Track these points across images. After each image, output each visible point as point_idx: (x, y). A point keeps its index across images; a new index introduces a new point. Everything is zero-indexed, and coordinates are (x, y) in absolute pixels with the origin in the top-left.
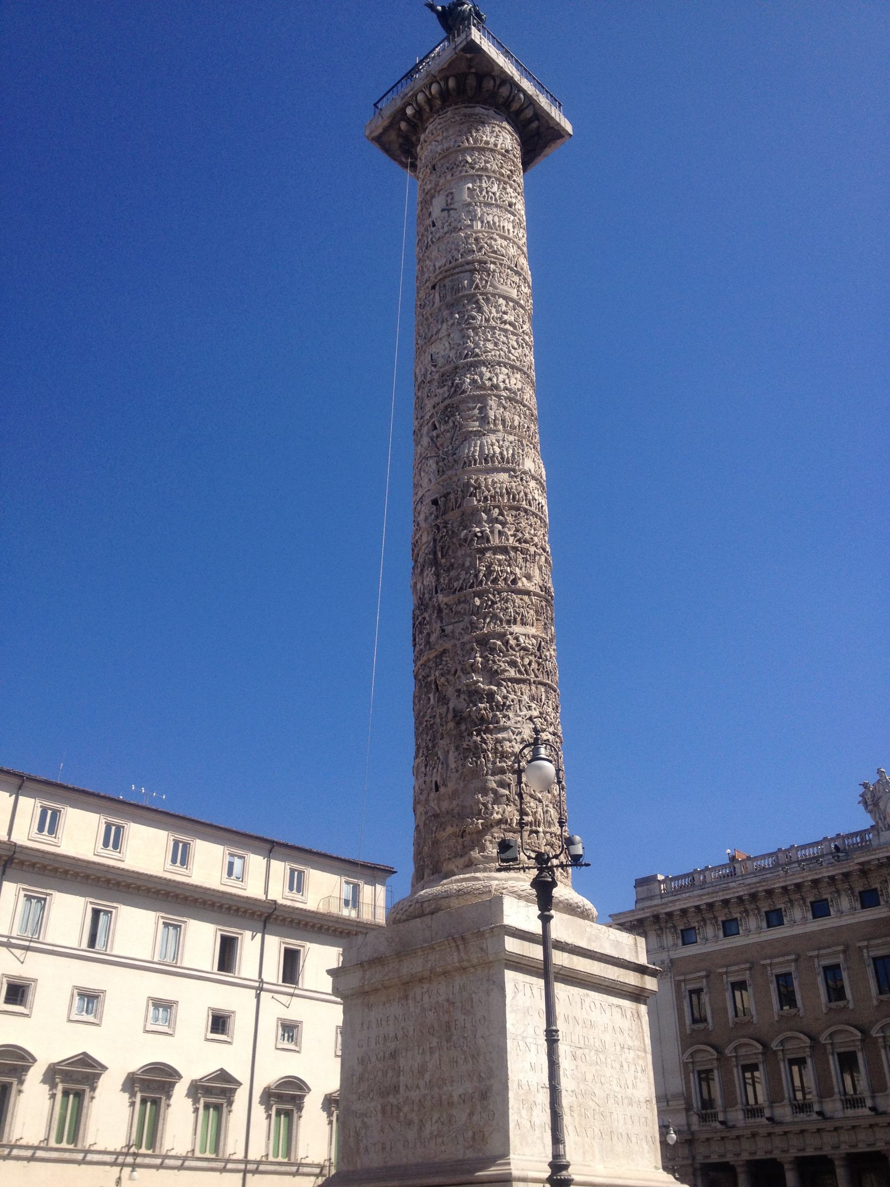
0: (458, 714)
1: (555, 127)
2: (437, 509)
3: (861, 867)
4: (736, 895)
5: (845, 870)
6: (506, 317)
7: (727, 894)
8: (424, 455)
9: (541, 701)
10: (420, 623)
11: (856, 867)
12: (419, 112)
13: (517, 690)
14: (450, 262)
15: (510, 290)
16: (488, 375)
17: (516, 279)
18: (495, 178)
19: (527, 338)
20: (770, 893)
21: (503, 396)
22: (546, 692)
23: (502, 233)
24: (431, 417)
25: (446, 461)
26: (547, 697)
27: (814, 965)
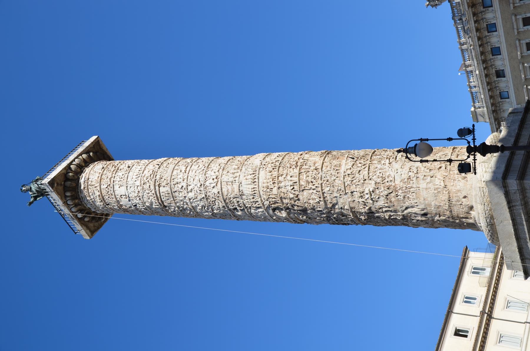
0: (386, 202)
1: (94, 144)
3: (470, 7)
4: (483, 70)
5: (472, 15)
6: (183, 171)
7: (482, 75)
8: (249, 215)
9: (381, 158)
10: (337, 221)
11: (470, 9)
12: (81, 211)
13: (375, 170)
14: (154, 198)
15: (170, 168)
16: (211, 181)
17: (165, 165)
18: (115, 174)
19: (194, 161)
20: (482, 53)
22: (376, 155)
23: (142, 171)
25: (253, 203)
26: (378, 155)
27: (522, 31)
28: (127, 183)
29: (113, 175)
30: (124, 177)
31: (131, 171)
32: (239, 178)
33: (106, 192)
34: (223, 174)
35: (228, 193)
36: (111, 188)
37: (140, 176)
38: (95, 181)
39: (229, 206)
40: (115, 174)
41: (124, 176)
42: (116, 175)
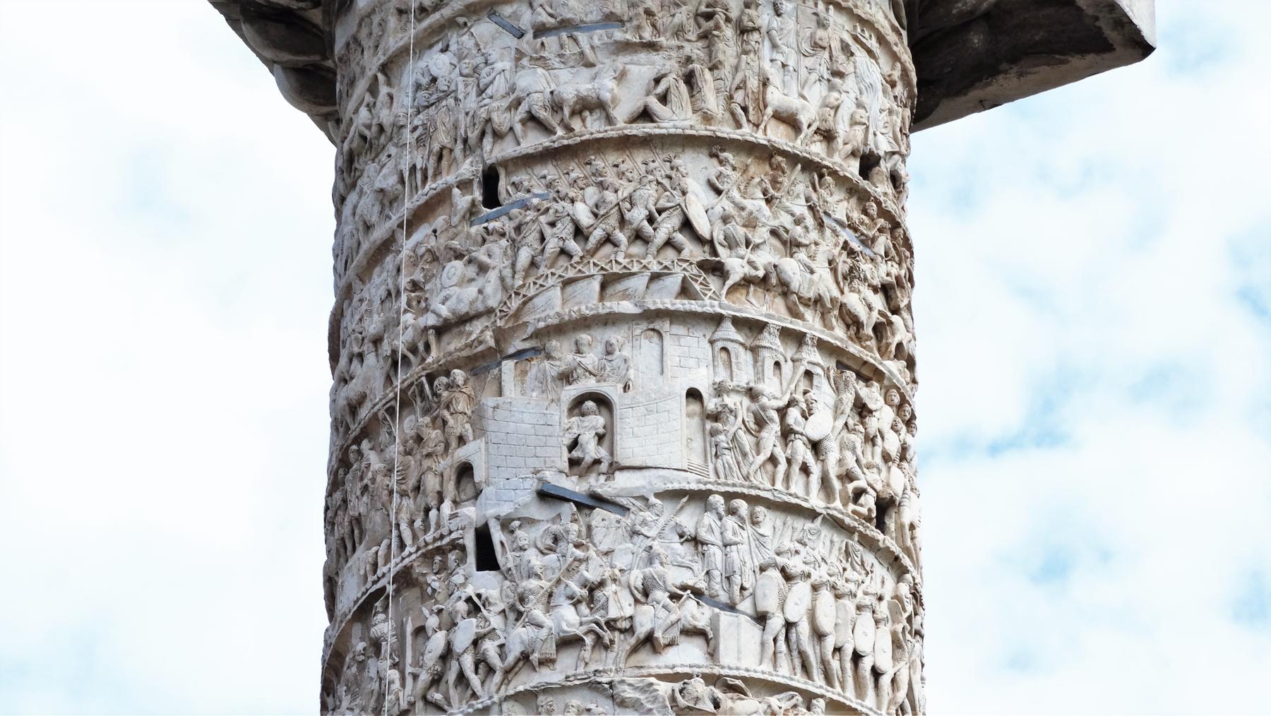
18: (822, 345)
28: (742, 505)
29: (811, 324)
30: (796, 468)
31: (854, 544)
33: (638, 216)
36: (685, 291)
37: (806, 668)
38: (753, 83)
40: (822, 345)
41: (805, 469)
42: (812, 355)
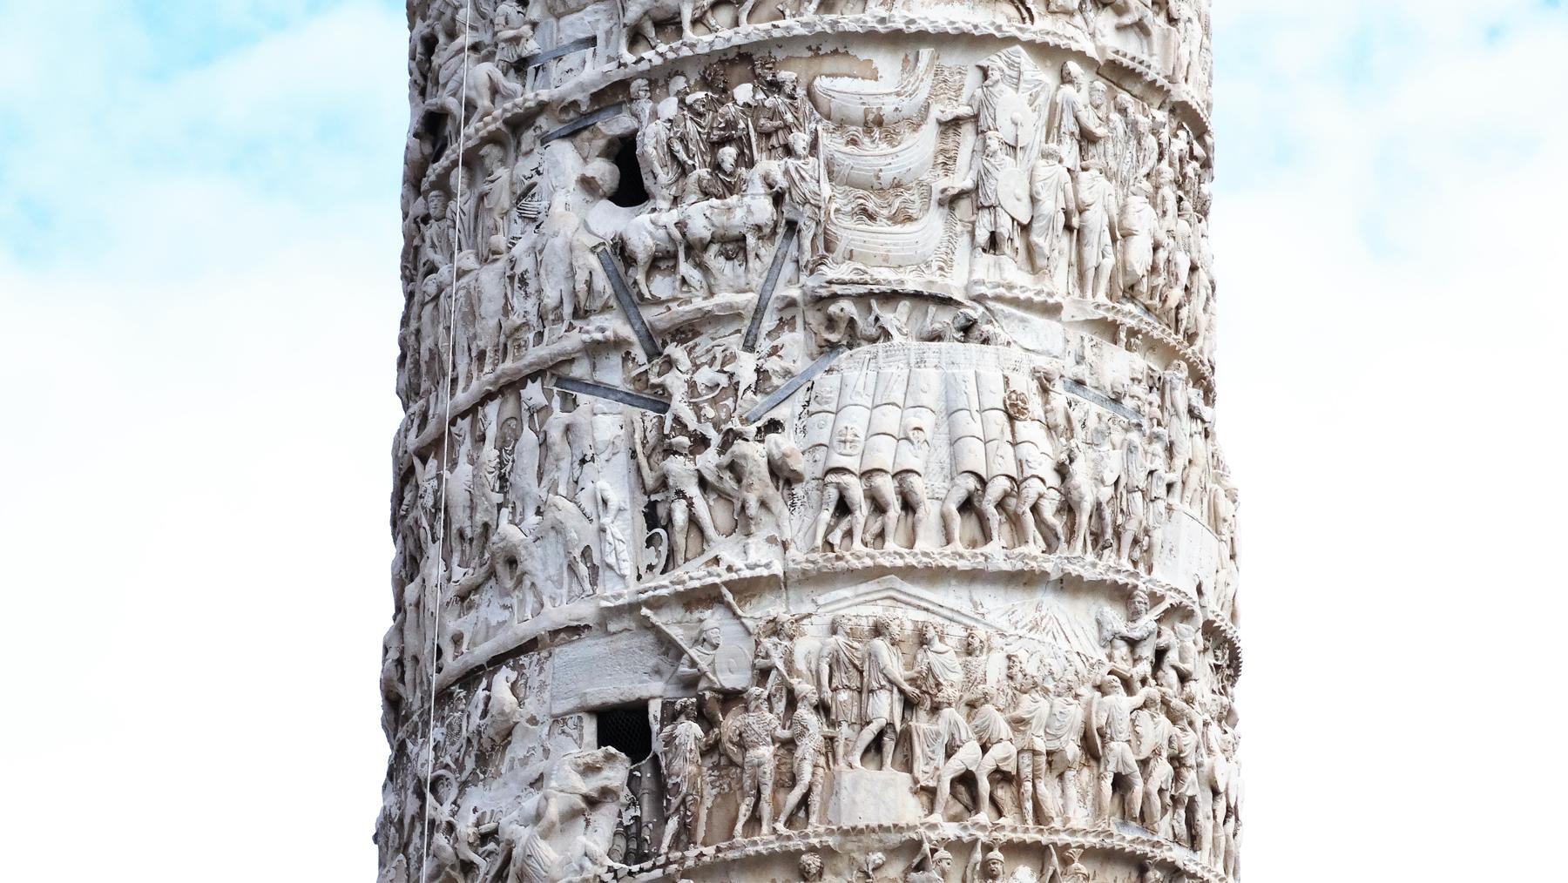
2: (632, 780)
21: (1081, 56)
24: (613, 95)
25: (709, 460)
32: (1028, 305)
34: (1073, 67)
35: (841, 124)
39: (669, 107)
